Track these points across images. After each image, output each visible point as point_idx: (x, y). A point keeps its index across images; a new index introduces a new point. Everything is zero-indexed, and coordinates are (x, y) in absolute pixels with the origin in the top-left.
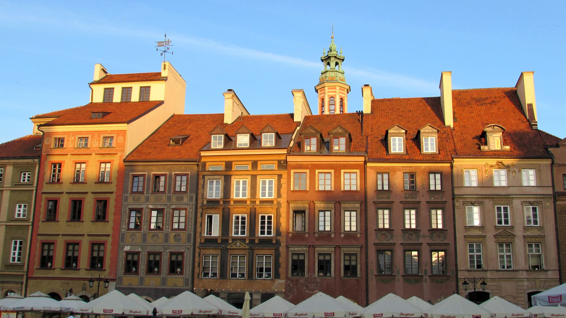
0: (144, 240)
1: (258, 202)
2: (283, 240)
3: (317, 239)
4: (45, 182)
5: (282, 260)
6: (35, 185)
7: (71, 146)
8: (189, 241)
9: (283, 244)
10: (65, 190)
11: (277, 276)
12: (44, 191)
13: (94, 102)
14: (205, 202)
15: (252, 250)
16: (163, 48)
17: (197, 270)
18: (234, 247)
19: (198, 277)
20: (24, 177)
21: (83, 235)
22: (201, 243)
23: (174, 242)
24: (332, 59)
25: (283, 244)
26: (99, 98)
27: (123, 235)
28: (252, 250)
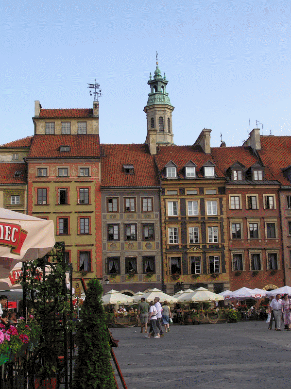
0: (122, 248)
1: (206, 218)
2: (226, 244)
3: (249, 244)
4: (33, 204)
5: (226, 259)
6: (25, 207)
7: (54, 175)
8: (157, 248)
9: (227, 248)
10: (52, 211)
11: (224, 271)
12: (33, 211)
13: (37, 133)
14: (167, 218)
15: (204, 253)
16: (93, 90)
17: (165, 269)
18: (192, 251)
19: (167, 274)
20: (14, 200)
21: (71, 246)
22: (166, 249)
23: (146, 249)
24: (159, 83)
25: (227, 248)
26: (41, 131)
27: (105, 245)
28: (204, 253)
